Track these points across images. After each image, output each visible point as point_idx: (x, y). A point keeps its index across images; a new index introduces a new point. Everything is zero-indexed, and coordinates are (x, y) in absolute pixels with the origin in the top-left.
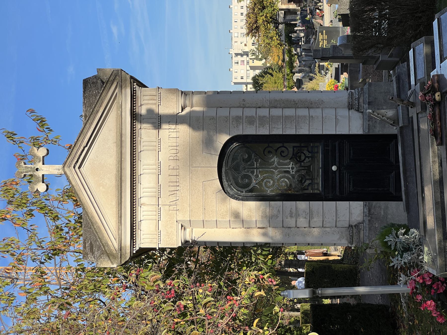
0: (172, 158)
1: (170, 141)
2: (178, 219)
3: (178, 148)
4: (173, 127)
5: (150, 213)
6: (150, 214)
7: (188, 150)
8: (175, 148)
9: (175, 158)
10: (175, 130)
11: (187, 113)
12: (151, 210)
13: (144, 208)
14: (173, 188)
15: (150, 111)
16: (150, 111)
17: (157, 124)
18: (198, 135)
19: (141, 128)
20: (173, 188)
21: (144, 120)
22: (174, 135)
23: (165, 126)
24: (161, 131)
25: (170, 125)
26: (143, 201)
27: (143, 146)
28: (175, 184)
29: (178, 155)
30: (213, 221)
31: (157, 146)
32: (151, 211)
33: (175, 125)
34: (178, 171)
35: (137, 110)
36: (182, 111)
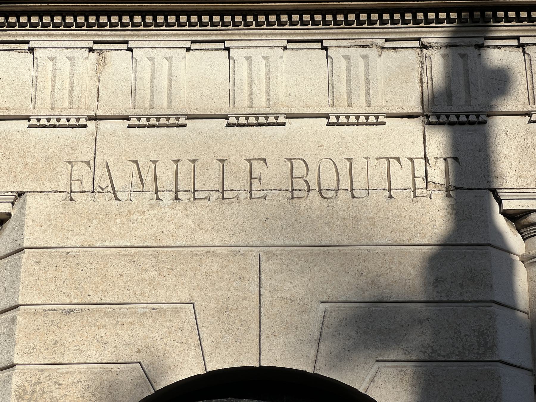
0: (299, 170)
1: (373, 162)
2: (30, 199)
3: (344, 195)
4: (438, 174)
5: (63, 84)
6: (58, 84)
7: (336, 239)
8: (345, 184)
9: (300, 184)
10: (420, 183)
11: (499, 235)
12: (77, 88)
13: (87, 62)
14: (166, 176)
15: (501, 81)
16: (501, 81)
17: (446, 108)
18: (406, 275)
19: (423, 47)
20: (166, 176)
21: (460, 61)
22: (401, 178)
23: (438, 141)
24: (415, 127)
25: (441, 164)
26: (118, 59)
27: (347, 58)
28: (185, 184)
29: (314, 195)
30: (11, 352)
31: (350, 110)
32: (71, 91)
33: (442, 181)
34: (243, 195)
35: (502, 30)
36: (506, 214)
